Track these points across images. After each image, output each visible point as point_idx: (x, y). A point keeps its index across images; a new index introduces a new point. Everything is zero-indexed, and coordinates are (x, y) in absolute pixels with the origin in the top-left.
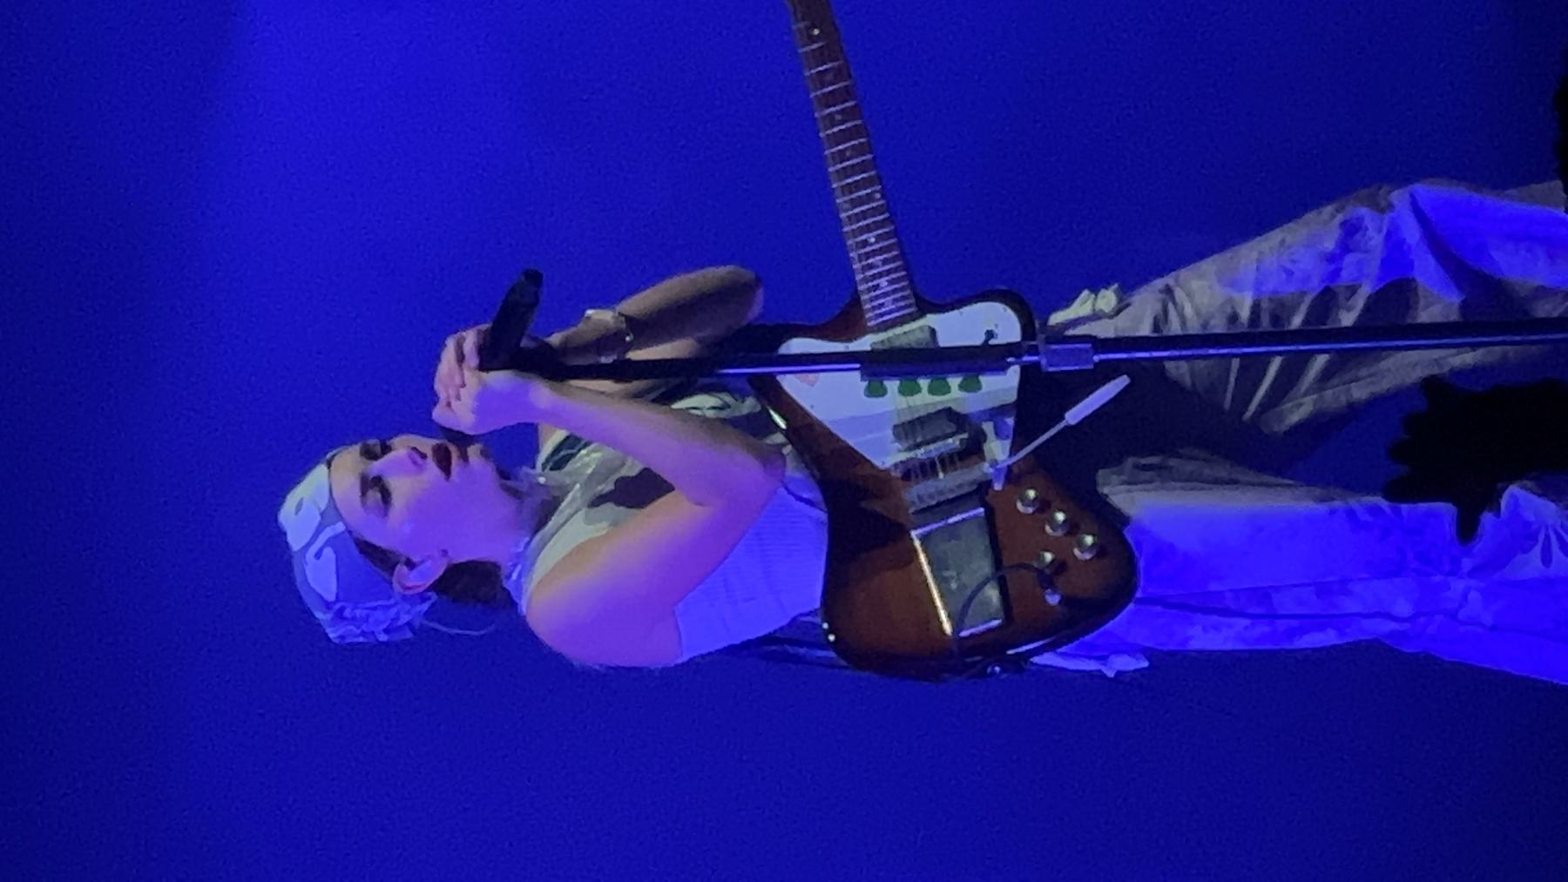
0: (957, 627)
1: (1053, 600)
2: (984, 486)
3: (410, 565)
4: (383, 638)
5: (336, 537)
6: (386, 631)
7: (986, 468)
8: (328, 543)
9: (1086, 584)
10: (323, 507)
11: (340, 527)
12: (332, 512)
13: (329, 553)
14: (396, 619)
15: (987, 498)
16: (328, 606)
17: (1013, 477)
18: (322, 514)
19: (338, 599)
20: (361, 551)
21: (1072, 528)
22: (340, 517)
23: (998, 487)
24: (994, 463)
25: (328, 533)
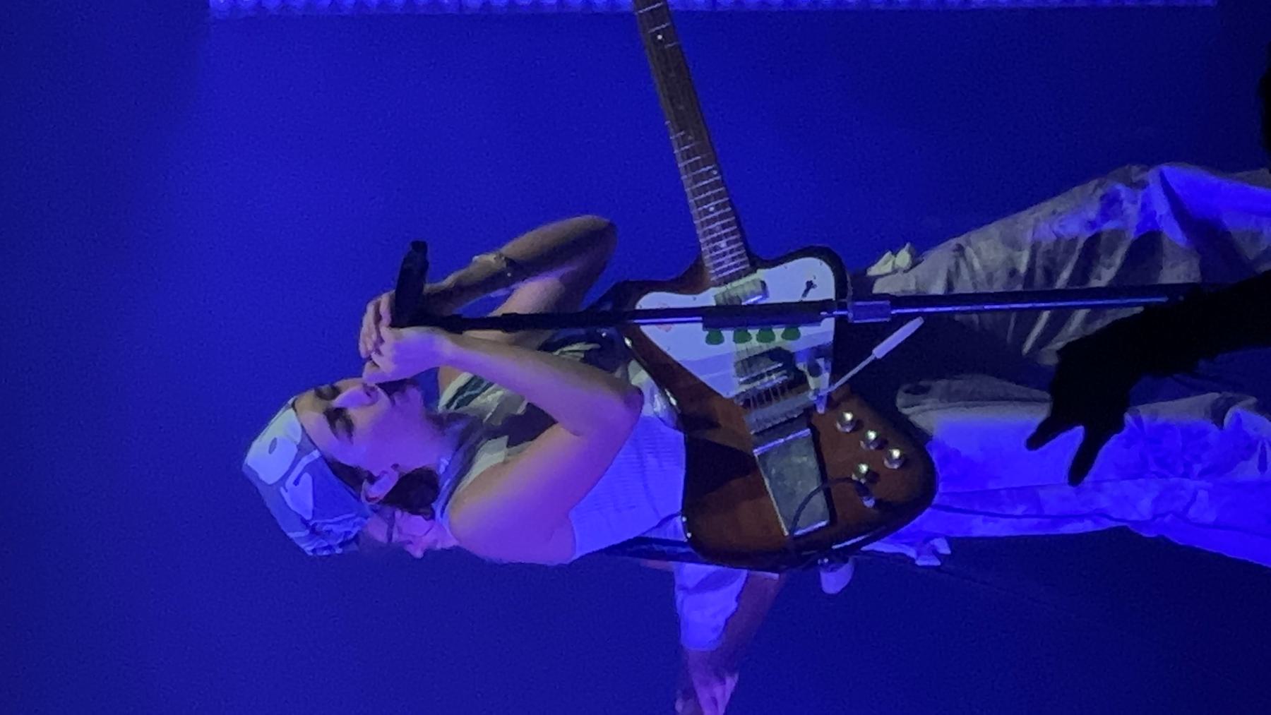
0: (791, 531)
2: (809, 411)
3: (372, 479)
4: (339, 551)
6: (341, 545)
8: (305, 470)
10: (298, 440)
11: (316, 454)
13: (307, 478)
15: (813, 421)
17: (833, 403)
18: (299, 447)
20: (335, 472)
21: (882, 444)
22: (316, 447)
23: (821, 410)
25: (305, 460)
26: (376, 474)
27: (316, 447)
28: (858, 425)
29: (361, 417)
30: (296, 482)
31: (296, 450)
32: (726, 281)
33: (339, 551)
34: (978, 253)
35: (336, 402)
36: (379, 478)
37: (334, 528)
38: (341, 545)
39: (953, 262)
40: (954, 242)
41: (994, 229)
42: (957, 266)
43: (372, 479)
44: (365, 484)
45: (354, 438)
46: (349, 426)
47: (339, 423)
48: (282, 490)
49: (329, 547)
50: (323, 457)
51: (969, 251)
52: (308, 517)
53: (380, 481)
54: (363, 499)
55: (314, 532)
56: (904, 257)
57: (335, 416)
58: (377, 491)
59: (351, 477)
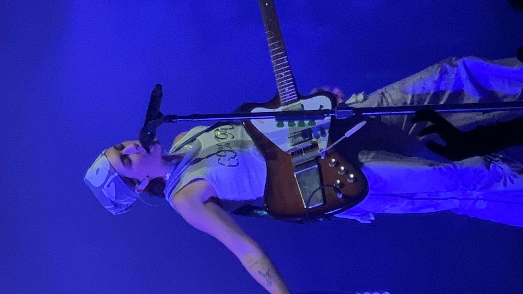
1: (340, 196)
4: (125, 212)
5: (116, 177)
7: (319, 152)
8: (113, 180)
9: (352, 192)
10: (108, 169)
11: (116, 174)
12: (112, 169)
13: (113, 184)
14: (128, 205)
15: (320, 162)
16: (112, 202)
17: (328, 154)
19: (116, 198)
21: (347, 172)
22: (116, 172)
23: (322, 158)
24: (321, 150)
25: (112, 177)
26: (140, 180)
27: (116, 172)
28: (337, 164)
29: (134, 157)
30: (109, 186)
31: (107, 173)
32: (287, 104)
33: (125, 212)
34: (390, 96)
35: (124, 152)
36: (142, 182)
37: (124, 203)
38: (125, 210)
39: (380, 99)
40: (380, 91)
41: (396, 85)
42: (382, 101)
43: (139, 183)
44: (137, 185)
45: (133, 167)
46: (130, 161)
47: (125, 160)
48: (102, 189)
49: (122, 211)
50: (119, 175)
51: (387, 95)
52: (114, 200)
53: (142, 184)
54: (136, 191)
55: (116, 205)
56: (361, 97)
57: (124, 158)
58: (141, 187)
59: (131, 182)
